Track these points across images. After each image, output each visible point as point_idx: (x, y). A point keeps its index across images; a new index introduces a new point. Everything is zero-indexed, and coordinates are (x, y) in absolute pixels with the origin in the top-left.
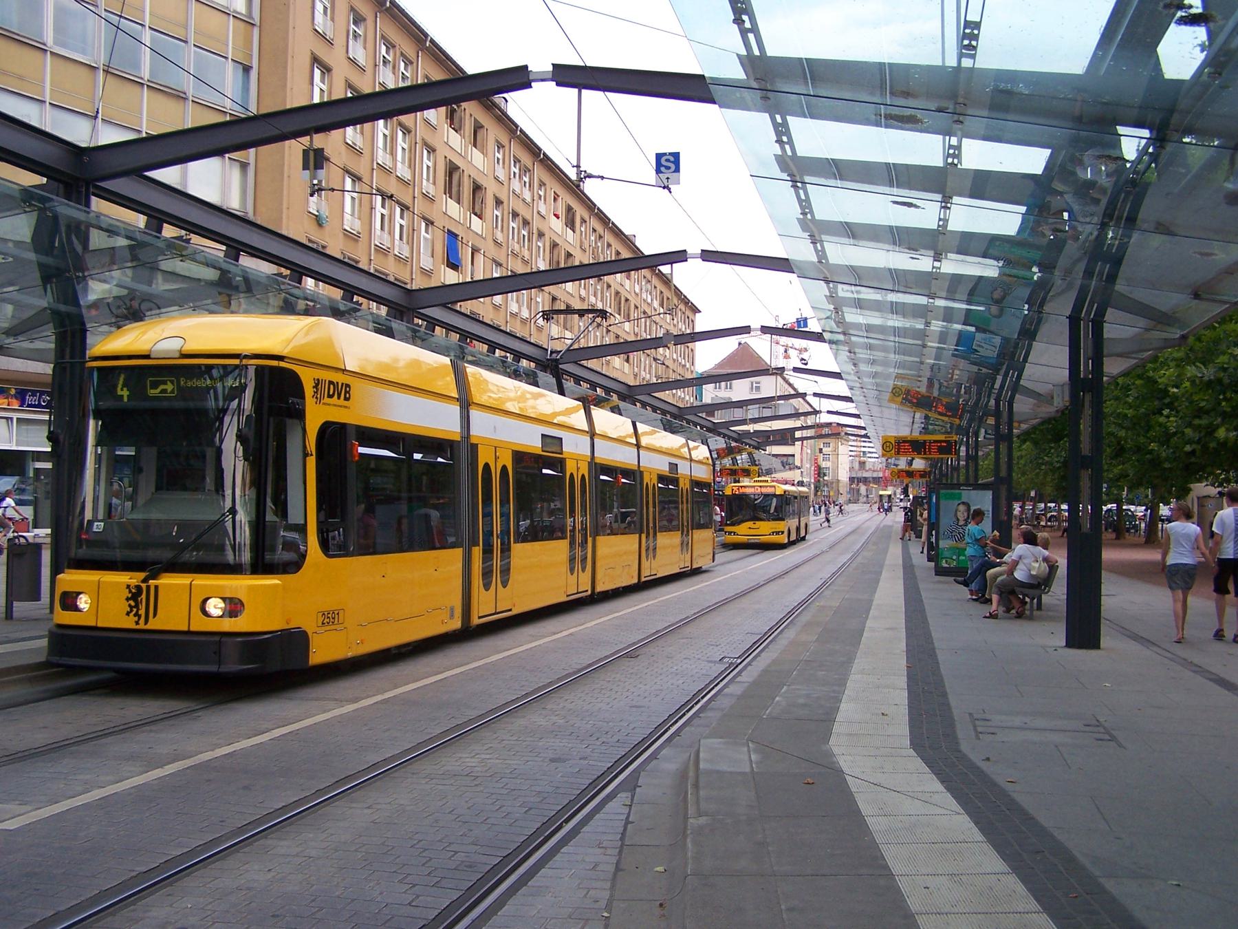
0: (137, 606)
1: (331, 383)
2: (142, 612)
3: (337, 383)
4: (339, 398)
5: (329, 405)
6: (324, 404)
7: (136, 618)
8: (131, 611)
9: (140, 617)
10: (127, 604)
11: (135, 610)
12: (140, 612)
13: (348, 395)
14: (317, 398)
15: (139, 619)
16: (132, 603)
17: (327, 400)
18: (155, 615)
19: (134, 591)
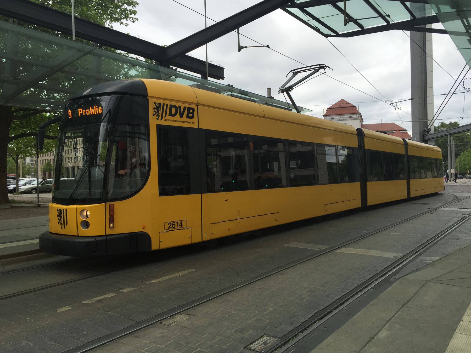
1: (172, 106)
2: (62, 222)
3: (180, 107)
4: (181, 116)
14: (158, 116)
16: (59, 217)
17: (168, 117)
18: (67, 224)
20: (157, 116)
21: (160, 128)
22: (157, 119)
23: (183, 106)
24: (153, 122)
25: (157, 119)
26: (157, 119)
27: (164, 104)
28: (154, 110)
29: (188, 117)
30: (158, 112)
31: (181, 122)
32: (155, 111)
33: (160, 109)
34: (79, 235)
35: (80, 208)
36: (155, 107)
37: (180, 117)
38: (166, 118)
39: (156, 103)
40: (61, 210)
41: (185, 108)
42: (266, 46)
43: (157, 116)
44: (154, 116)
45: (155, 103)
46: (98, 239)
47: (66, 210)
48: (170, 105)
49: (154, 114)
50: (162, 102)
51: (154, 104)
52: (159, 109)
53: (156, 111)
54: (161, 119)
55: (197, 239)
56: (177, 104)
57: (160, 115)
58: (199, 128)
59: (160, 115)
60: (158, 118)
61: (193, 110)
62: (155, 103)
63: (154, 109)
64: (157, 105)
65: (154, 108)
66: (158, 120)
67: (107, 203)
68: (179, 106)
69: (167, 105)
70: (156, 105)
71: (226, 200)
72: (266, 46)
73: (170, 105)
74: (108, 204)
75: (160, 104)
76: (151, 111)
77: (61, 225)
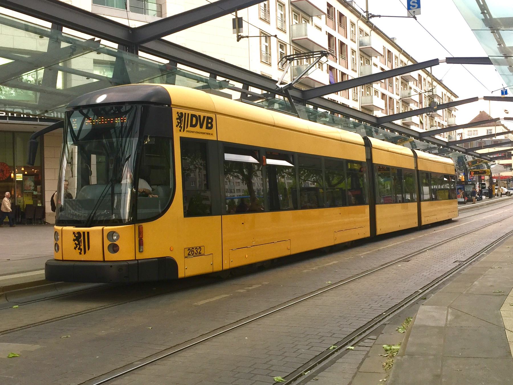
0: (79, 244)
1: (193, 116)
2: (82, 247)
3: (200, 116)
4: (201, 127)
5: (193, 132)
6: (187, 131)
7: (80, 251)
8: (77, 247)
9: (81, 250)
10: (74, 243)
11: (78, 246)
12: (81, 247)
13: (209, 125)
14: (181, 127)
15: (81, 251)
16: (77, 243)
17: (190, 129)
18: (89, 249)
19: (77, 235)
21: (183, 140)
22: (180, 131)
23: (202, 114)
24: (177, 135)
25: (180, 131)
27: (185, 114)
29: (207, 128)
30: (181, 123)
31: (201, 133)
34: (105, 260)
35: (107, 230)
37: (200, 128)
38: (187, 130)
40: (81, 233)
41: (204, 117)
42: (274, 36)
43: (180, 127)
46: (130, 263)
47: (88, 233)
48: (191, 114)
50: (184, 111)
54: (184, 131)
55: (217, 268)
56: (197, 113)
57: (182, 125)
58: (218, 140)
59: (182, 125)
61: (211, 119)
63: (177, 119)
67: (136, 224)
68: (199, 116)
69: (188, 114)
71: (243, 223)
72: (274, 36)
73: (191, 114)
74: (137, 225)
75: (182, 113)
76: (175, 122)
77: (80, 250)
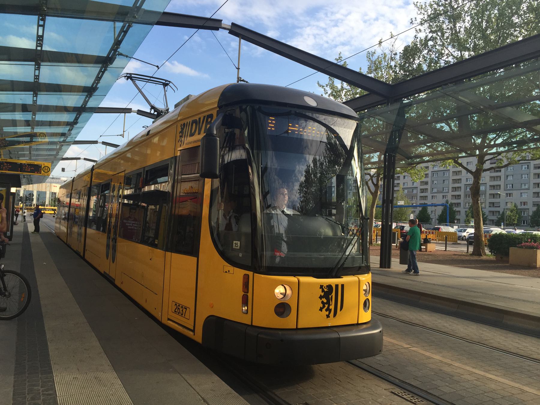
14: (329, 310)
20: (326, 310)
22: (328, 316)
25: (328, 316)
26: (327, 315)
27: (337, 286)
28: (321, 299)
30: (328, 303)
32: (323, 302)
33: (332, 297)
36: (323, 294)
39: (323, 286)
43: (326, 310)
44: (322, 311)
45: (321, 287)
49: (321, 307)
51: (320, 288)
52: (330, 296)
53: (325, 301)
57: (332, 307)
59: (332, 307)
60: (330, 313)
62: (321, 287)
63: (321, 297)
64: (326, 290)
65: (321, 295)
66: (329, 317)
70: (323, 291)
75: (330, 287)
